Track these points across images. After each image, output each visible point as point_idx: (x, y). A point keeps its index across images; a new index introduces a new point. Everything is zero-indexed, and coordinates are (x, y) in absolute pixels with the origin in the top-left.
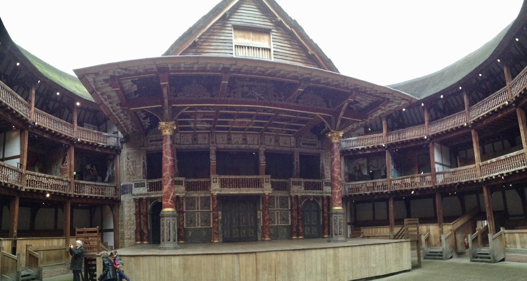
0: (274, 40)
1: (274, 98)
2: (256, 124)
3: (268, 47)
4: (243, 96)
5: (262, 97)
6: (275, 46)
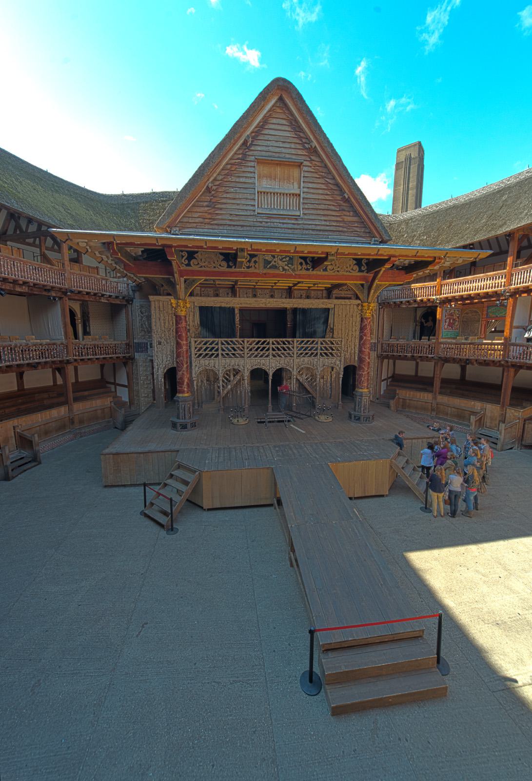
1: (300, 267)
3: (297, 192)
4: (265, 267)
6: (305, 190)
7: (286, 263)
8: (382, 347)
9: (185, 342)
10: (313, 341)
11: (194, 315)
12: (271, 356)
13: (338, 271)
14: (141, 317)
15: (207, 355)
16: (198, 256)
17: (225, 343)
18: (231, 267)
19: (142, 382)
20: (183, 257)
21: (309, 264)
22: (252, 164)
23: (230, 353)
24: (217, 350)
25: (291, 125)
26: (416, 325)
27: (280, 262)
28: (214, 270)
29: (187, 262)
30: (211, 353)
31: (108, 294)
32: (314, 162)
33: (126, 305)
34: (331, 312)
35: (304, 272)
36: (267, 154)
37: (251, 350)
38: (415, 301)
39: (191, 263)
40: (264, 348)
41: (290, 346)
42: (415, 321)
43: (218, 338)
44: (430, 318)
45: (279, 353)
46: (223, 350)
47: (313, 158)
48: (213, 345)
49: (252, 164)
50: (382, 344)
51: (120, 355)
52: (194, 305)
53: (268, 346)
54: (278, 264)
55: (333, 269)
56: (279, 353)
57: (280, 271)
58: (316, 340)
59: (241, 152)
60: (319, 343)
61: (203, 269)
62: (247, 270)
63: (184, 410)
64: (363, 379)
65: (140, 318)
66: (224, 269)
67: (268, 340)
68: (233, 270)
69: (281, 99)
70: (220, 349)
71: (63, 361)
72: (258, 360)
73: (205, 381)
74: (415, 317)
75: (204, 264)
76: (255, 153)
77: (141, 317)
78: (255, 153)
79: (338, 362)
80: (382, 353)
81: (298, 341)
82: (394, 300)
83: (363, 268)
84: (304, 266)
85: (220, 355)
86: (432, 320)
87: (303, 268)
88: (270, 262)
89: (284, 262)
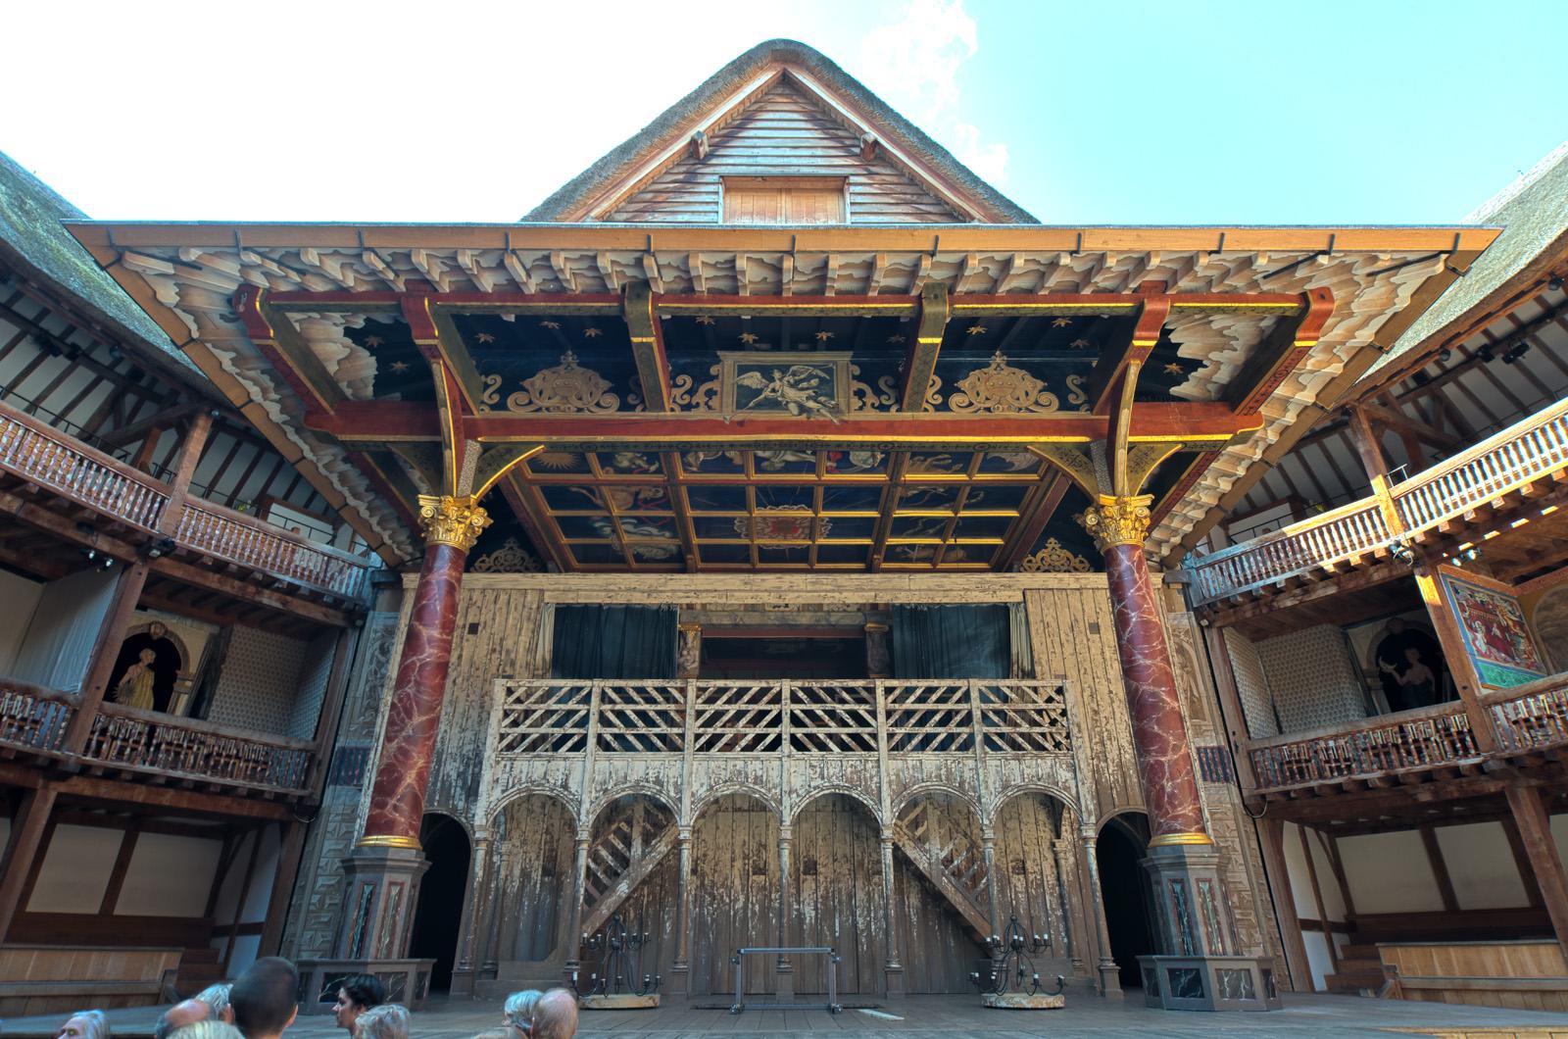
0: (857, 209)
1: (856, 402)
2: (840, 527)
5: (811, 404)
7: (811, 392)
8: (1253, 766)
9: (436, 633)
10: (952, 690)
11: (535, 632)
12: (786, 747)
13: (988, 409)
14: (379, 662)
15: (543, 738)
16: (532, 384)
17: (614, 696)
18: (632, 408)
19: (315, 899)
20: (487, 386)
21: (885, 393)
22: (712, 188)
23: (629, 734)
24: (583, 722)
25: (812, 119)
26: (1367, 690)
27: (791, 393)
28: (580, 415)
29: (496, 398)
30: (558, 732)
31: (288, 579)
32: (878, 178)
33: (342, 632)
34: (1016, 619)
35: (871, 415)
36: (753, 169)
37: (708, 723)
38: (1321, 573)
39: (510, 401)
40: (762, 714)
41: (862, 709)
42: (1357, 673)
43: (590, 678)
44: (1412, 655)
45: (818, 709)
46: (604, 721)
47: (873, 169)
48: (571, 705)
49: (712, 188)
50: (1250, 754)
51: (265, 787)
52: (541, 599)
53: (775, 709)
54: (783, 396)
55: (971, 404)
56: (821, 732)
57: (792, 414)
58: (962, 683)
59: (683, 169)
60: (974, 695)
61: (544, 414)
62: (685, 413)
63: (367, 913)
64: (1168, 786)
65: (374, 666)
66: (611, 411)
67: (776, 685)
68: (637, 415)
69: (786, 82)
70: (594, 718)
71: (35, 756)
72: (737, 759)
73: (537, 876)
74: (1353, 659)
75: (546, 403)
76: (718, 169)
77: (379, 662)
78: (718, 169)
79: (1064, 775)
80: (1263, 791)
81: (889, 691)
82: (1245, 588)
83: (1071, 398)
84: (870, 399)
85: (592, 741)
86: (1421, 661)
87: (869, 405)
88: (759, 392)
89: (803, 389)
